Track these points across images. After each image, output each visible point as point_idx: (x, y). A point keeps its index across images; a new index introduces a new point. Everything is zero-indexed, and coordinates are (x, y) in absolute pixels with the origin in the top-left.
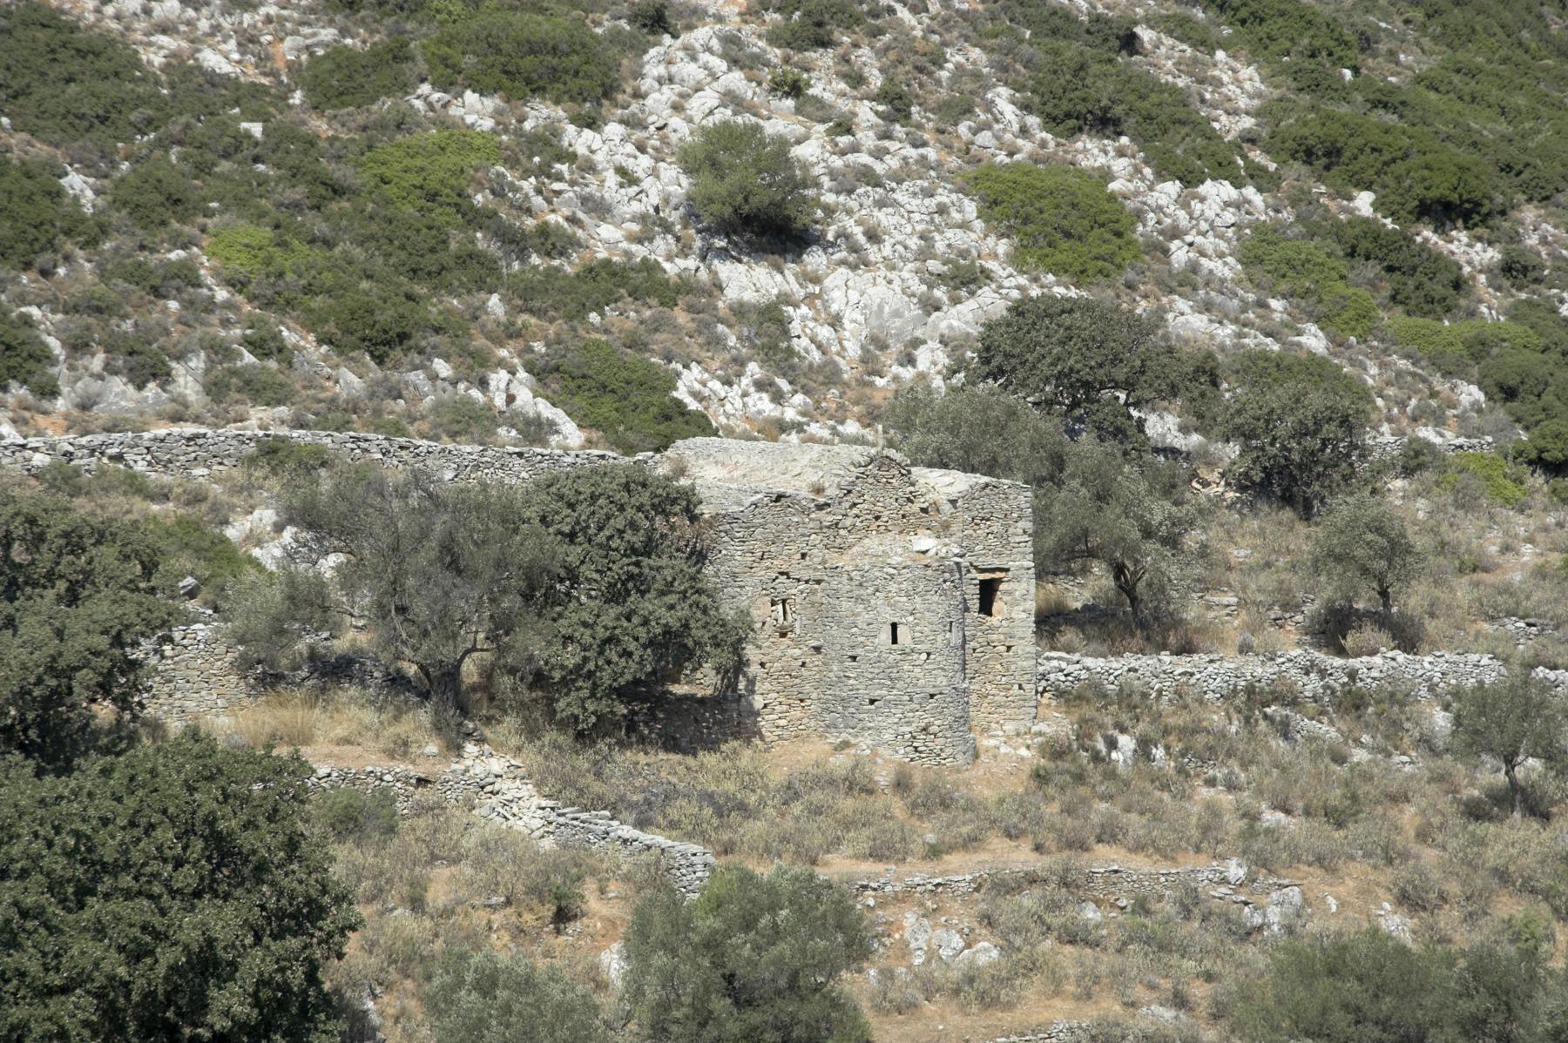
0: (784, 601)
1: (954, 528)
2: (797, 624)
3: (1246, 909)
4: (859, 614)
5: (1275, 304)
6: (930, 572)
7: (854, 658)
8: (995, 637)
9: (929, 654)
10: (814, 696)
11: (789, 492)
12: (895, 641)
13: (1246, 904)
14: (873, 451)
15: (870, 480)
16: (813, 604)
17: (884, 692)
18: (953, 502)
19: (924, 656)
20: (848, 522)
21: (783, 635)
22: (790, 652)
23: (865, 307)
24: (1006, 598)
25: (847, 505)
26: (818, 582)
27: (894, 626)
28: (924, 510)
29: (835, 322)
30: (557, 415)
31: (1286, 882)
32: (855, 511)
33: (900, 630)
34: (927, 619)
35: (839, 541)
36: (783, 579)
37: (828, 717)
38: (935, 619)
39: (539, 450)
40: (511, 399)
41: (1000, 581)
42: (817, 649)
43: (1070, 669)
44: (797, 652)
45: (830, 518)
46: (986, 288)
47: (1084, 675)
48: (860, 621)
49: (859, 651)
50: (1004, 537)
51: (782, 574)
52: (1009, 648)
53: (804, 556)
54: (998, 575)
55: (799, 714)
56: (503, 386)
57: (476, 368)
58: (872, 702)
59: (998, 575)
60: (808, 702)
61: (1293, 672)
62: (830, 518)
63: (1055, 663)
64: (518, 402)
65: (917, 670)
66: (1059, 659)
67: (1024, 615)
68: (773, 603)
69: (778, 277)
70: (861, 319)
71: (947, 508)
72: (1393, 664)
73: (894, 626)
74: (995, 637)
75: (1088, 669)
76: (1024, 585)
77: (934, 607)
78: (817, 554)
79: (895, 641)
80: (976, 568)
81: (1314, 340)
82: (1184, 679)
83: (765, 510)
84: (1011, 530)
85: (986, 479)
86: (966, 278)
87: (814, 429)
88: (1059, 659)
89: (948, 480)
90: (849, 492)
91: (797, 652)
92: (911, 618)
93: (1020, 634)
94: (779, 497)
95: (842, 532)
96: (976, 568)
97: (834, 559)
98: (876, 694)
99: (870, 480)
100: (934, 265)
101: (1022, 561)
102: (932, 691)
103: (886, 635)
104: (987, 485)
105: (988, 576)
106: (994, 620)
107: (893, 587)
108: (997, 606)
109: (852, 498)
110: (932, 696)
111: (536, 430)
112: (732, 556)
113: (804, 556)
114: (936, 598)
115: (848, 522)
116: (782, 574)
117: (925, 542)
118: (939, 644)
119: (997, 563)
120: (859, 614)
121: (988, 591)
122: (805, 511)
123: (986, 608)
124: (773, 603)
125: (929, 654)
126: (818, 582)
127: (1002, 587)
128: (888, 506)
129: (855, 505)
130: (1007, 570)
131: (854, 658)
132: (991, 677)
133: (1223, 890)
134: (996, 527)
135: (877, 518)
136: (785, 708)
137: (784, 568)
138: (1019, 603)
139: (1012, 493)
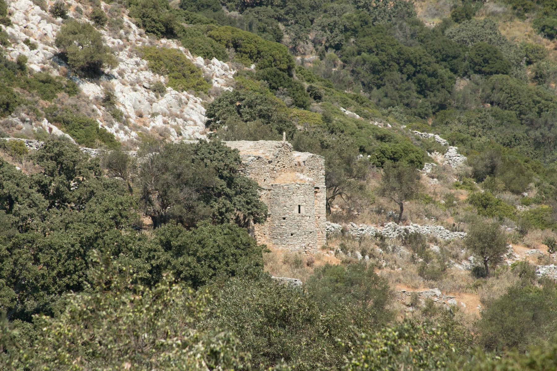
4: (287, 202)
7: (284, 219)
12: (299, 212)
17: (296, 231)
18: (304, 162)
26: (269, 190)
27: (299, 206)
32: (278, 164)
33: (301, 208)
40: (51, 129)
43: (328, 227)
45: (272, 166)
47: (333, 229)
48: (287, 205)
49: (287, 216)
53: (265, 180)
58: (292, 235)
62: (272, 166)
64: (53, 131)
65: (306, 223)
70: (131, 105)
71: (302, 164)
73: (299, 206)
79: (299, 212)
82: (361, 232)
85: (312, 154)
92: (305, 203)
95: (275, 172)
98: (293, 232)
102: (311, 231)
107: (299, 192)
120: (287, 202)
122: (265, 163)
126: (269, 190)
131: (284, 219)
134: (315, 172)
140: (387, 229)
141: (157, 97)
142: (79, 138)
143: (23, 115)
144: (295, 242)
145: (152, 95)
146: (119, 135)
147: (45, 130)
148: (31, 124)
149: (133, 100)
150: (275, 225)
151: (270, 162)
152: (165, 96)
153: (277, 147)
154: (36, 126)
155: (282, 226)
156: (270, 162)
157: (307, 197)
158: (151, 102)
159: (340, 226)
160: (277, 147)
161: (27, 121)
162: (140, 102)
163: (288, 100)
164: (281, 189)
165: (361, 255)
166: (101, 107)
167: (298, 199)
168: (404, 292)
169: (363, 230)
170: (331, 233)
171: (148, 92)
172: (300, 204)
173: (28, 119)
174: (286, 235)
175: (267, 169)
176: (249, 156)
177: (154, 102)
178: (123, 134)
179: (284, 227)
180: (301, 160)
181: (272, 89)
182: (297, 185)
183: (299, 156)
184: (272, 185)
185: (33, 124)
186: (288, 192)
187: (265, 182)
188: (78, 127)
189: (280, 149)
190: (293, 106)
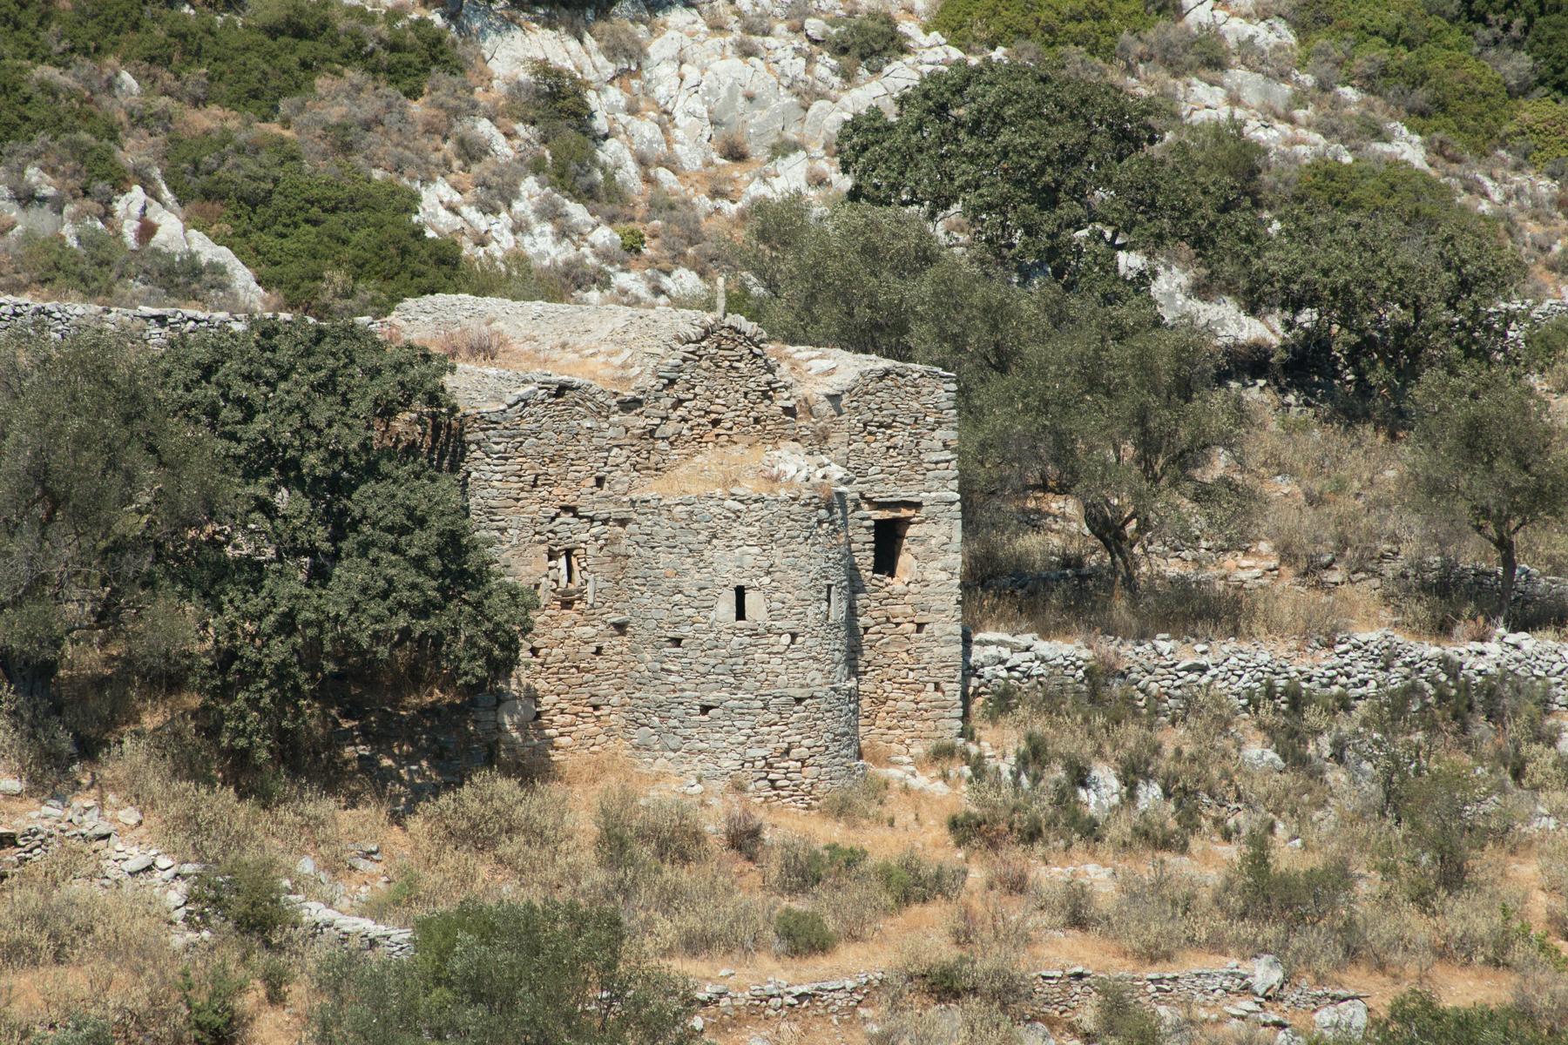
0: (569, 553)
1: (831, 443)
2: (589, 588)
3: (1281, 1035)
4: (685, 573)
5: (1349, 93)
6: (796, 508)
7: (677, 642)
8: (898, 609)
9: (794, 636)
10: (615, 700)
11: (577, 381)
12: (741, 615)
13: (1281, 1026)
14: (709, 318)
15: (705, 364)
16: (615, 556)
17: (724, 695)
18: (834, 398)
19: (786, 639)
20: (669, 429)
21: (567, 605)
22: (578, 631)
23: (710, 91)
24: (915, 549)
25: (669, 402)
26: (623, 522)
27: (740, 592)
28: (789, 411)
29: (666, 119)
30: (224, 255)
31: (1342, 992)
32: (681, 412)
33: (750, 598)
34: (791, 583)
35: (655, 458)
36: (566, 517)
37: (639, 735)
38: (804, 581)
39: (190, 312)
40: (147, 230)
41: (906, 522)
42: (621, 628)
43: (1016, 659)
44: (589, 631)
45: (641, 422)
46: (896, 64)
48: (688, 584)
49: (685, 630)
50: (914, 454)
51: (566, 509)
52: (920, 627)
53: (600, 482)
54: (904, 513)
55: (591, 728)
56: (136, 210)
57: (99, 178)
58: (705, 709)
59: (904, 513)
60: (605, 710)
61: (1361, 665)
62: (641, 422)
63: (992, 650)
65: (776, 660)
66: (1001, 643)
67: (944, 576)
68: (552, 556)
69: (573, 45)
70: (702, 110)
71: (825, 407)
72: (1518, 654)
73: (740, 592)
74: (898, 609)
75: (1043, 660)
76: (944, 528)
77: (803, 561)
78: (620, 480)
79: (741, 615)
80: (869, 501)
81: (1409, 148)
82: (1194, 676)
83: (539, 409)
84: (924, 444)
85: (887, 363)
86: (869, 44)
87: (622, 279)
88: (1001, 643)
89: (826, 364)
90: (672, 382)
91: (589, 631)
92: (766, 580)
93: (937, 605)
94: (562, 389)
95: (661, 445)
96: (869, 501)
97: (650, 489)
98: (710, 697)
99: (705, 364)
100: (814, 26)
101: (939, 491)
102: (799, 693)
103: (726, 607)
104: (887, 373)
105: (887, 514)
106: (897, 584)
107: (739, 530)
108: (905, 561)
109: (678, 391)
110: (799, 701)
111: (184, 278)
112: (489, 477)
113: (600, 482)
114: (804, 549)
115: (669, 429)
116: (566, 509)
117: (792, 462)
118: (810, 621)
119: (902, 494)
120: (685, 573)
121: (888, 539)
122: (601, 412)
123: (886, 562)
124: (552, 556)
125: (794, 636)
126: (623, 522)
127: (911, 531)
128: (731, 402)
129: (680, 402)
130: (918, 506)
131: (677, 642)
132: (891, 672)
133: (1246, 1004)
135: (715, 423)
136: (568, 718)
137: (569, 500)
138: (935, 559)
139: (927, 385)
140: (1347, 660)
141: (848, 76)
142: (277, 263)
143: (33, 174)
144: (716, 740)
145: (826, 65)
146: (527, 240)
147: (119, 234)
148: (60, 212)
149: (723, 93)
150: (642, 667)
151: (628, 406)
152: (887, 69)
153: (678, 338)
154: (76, 219)
155: (669, 671)
156: (628, 406)
157: (778, 552)
158: (807, 95)
159: (1086, 654)
160: (678, 338)
161: (43, 200)
162: (750, 98)
163: (1519, 64)
164: (664, 521)
165: (1115, 784)
166: (520, 127)
167: (733, 561)
168: (1079, 976)
169: (1203, 669)
170: (1026, 685)
171: (810, 59)
172: (744, 582)
173: (48, 191)
174: (679, 711)
175: (611, 433)
176: (526, 382)
177: (821, 96)
178: (550, 238)
179: (673, 678)
180: (816, 390)
181: (1476, 21)
182: (729, 503)
183: (831, 372)
184: (633, 502)
185: (69, 209)
186: (703, 529)
187: (605, 491)
188: (300, 216)
189: (691, 347)
190: (1542, 90)
